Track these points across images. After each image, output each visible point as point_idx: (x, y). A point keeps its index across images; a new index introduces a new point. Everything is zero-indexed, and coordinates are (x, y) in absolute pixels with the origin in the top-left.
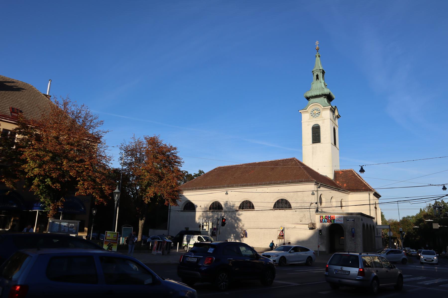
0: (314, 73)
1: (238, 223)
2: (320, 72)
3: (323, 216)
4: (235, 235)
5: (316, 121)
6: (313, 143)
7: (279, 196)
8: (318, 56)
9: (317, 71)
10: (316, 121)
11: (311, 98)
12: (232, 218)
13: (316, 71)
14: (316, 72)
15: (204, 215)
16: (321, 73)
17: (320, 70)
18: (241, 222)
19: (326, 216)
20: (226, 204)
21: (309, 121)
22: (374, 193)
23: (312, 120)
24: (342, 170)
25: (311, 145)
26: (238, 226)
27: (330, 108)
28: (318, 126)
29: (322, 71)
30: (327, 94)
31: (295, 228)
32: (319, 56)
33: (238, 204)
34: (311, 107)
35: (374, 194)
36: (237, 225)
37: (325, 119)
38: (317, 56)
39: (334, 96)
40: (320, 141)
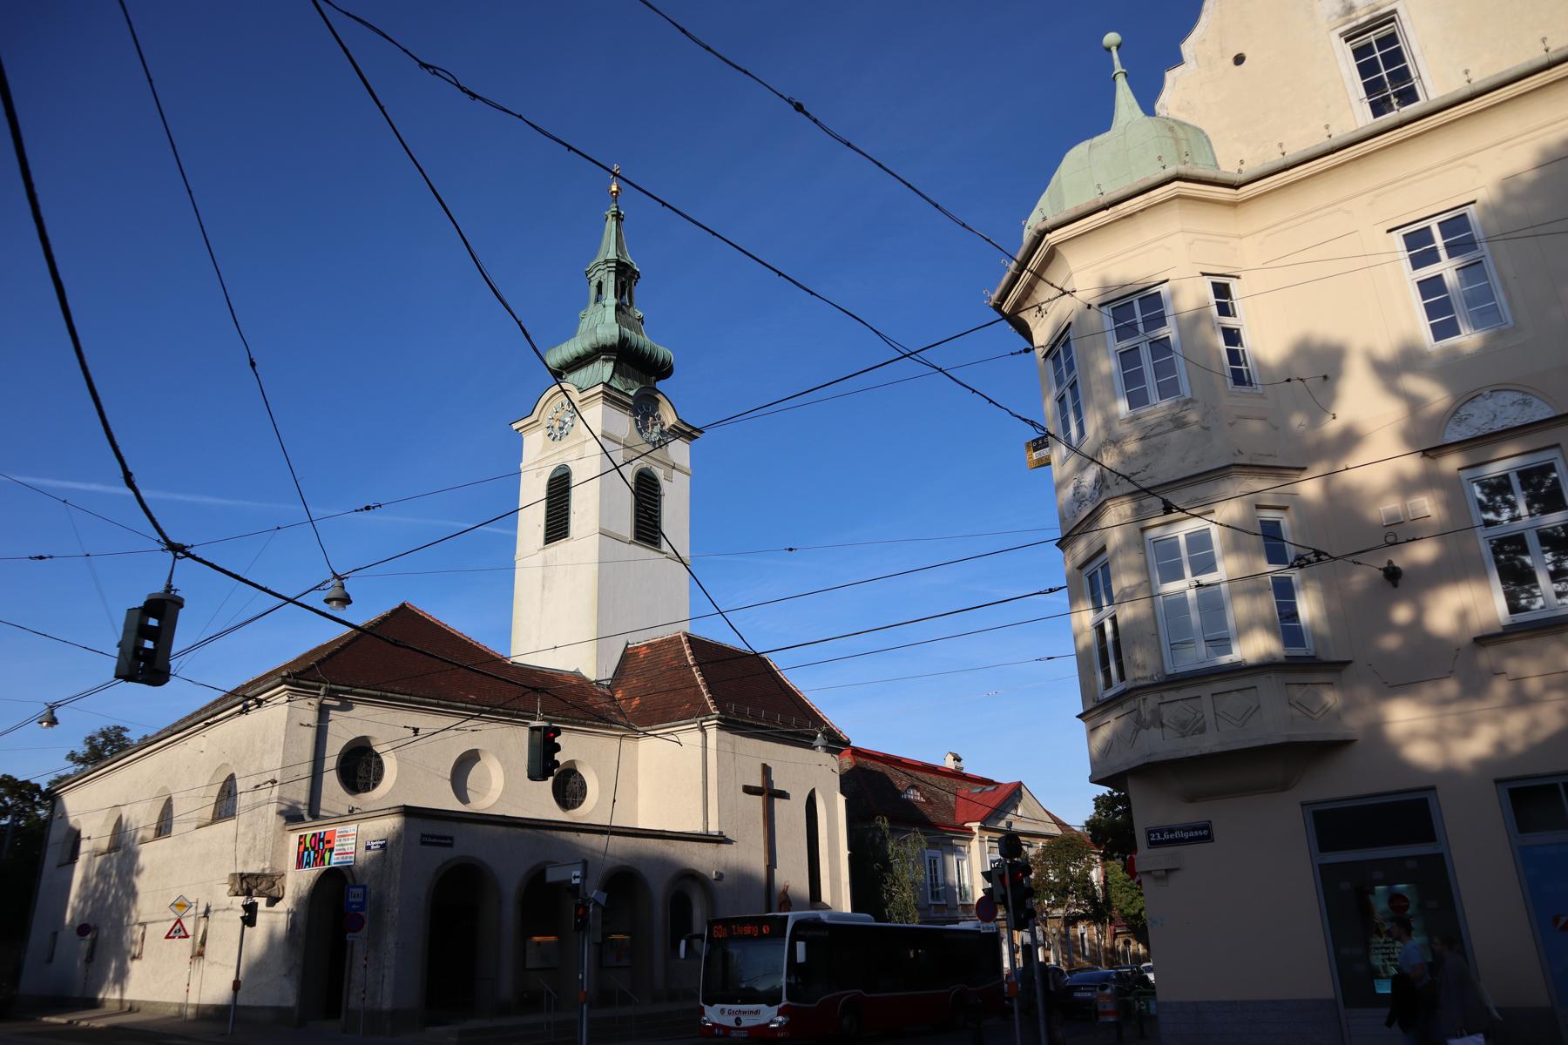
0: (592, 279)
2: (606, 271)
7: (220, 764)
8: (613, 216)
16: (612, 275)
17: (607, 261)
19: (314, 835)
21: (544, 456)
22: (715, 722)
23: (550, 453)
24: (651, 641)
25: (541, 553)
28: (566, 471)
29: (614, 265)
30: (609, 343)
34: (550, 402)
35: (720, 728)
37: (586, 441)
38: (610, 217)
39: (664, 352)
40: (567, 532)
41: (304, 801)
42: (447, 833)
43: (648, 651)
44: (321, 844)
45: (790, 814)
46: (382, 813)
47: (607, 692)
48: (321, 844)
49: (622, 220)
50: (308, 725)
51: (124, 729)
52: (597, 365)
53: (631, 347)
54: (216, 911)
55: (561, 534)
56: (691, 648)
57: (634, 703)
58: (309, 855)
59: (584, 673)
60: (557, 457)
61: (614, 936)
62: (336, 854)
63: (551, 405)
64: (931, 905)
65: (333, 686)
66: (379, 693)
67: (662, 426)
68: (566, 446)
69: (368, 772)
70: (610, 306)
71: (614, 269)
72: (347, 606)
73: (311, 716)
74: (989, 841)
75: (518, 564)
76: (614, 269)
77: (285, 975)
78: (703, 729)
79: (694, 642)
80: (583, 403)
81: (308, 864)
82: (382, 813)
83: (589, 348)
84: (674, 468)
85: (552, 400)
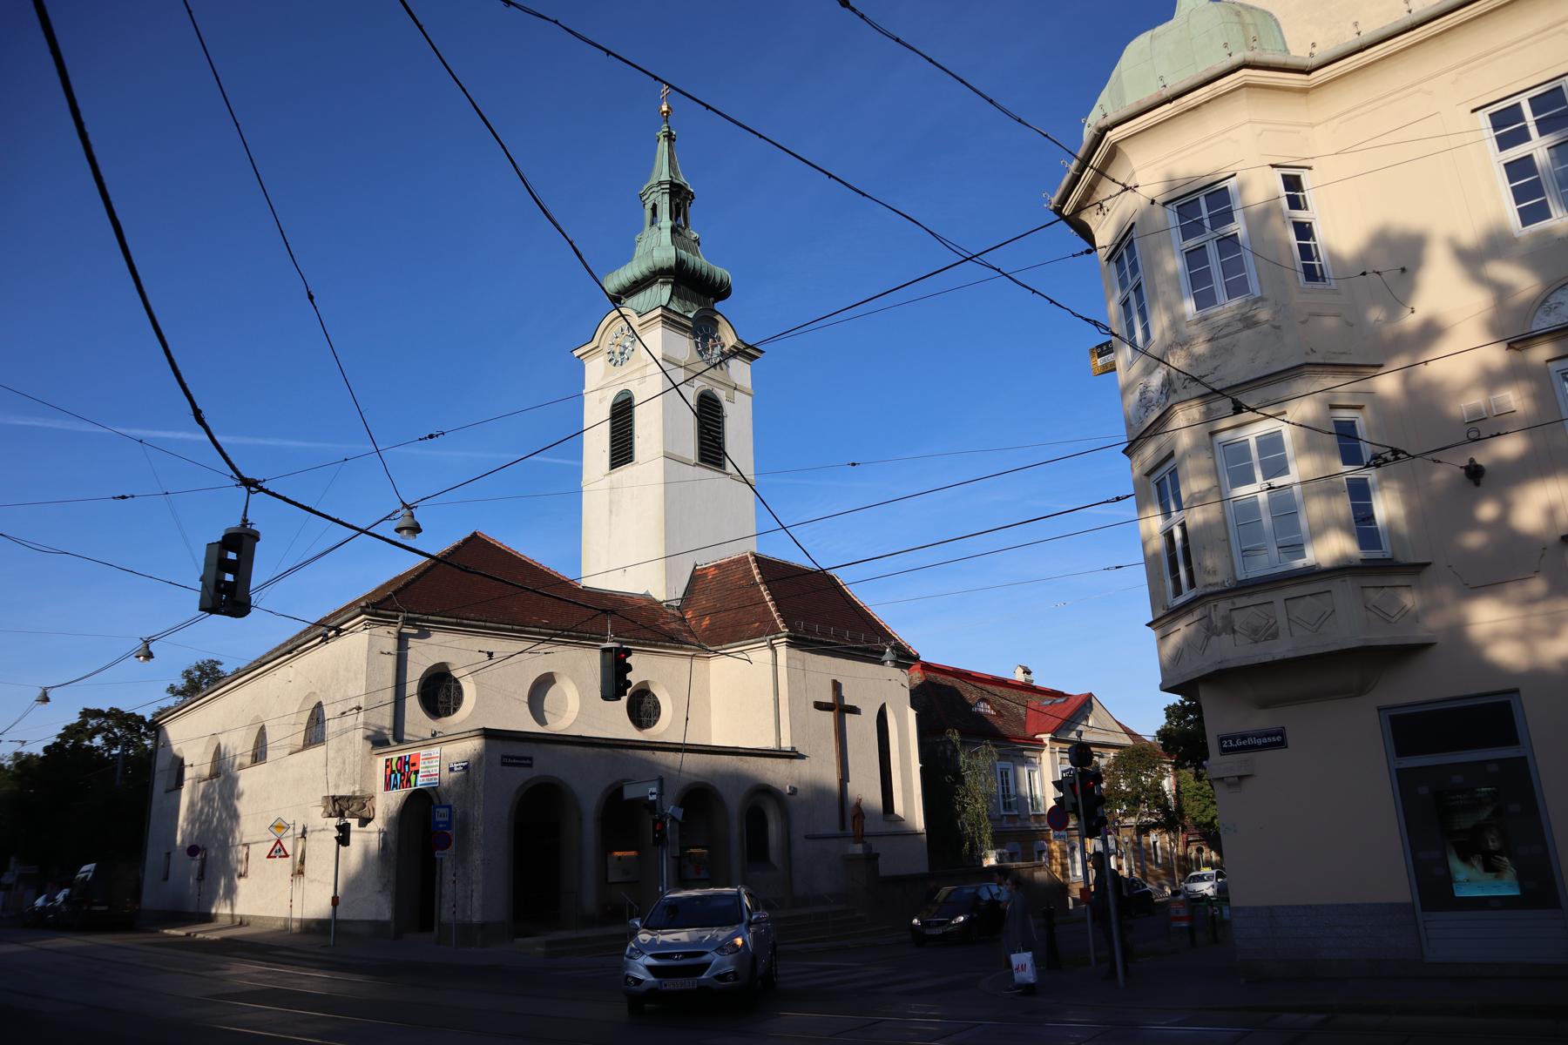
3: (392, 759)
6: (612, 469)
8: (664, 136)
9: (653, 189)
11: (626, 297)
13: (649, 193)
14: (652, 197)
16: (667, 197)
17: (660, 183)
19: (400, 758)
22: (785, 639)
27: (661, 315)
28: (628, 397)
30: (666, 265)
32: (670, 137)
34: (610, 327)
35: (790, 645)
38: (662, 137)
39: (721, 272)
41: (388, 726)
42: (527, 754)
43: (716, 572)
44: (407, 766)
45: (861, 729)
46: (463, 736)
47: (677, 613)
48: (407, 766)
49: (674, 140)
50: (389, 653)
51: (218, 663)
52: (655, 288)
53: (688, 269)
54: (312, 831)
55: (626, 459)
56: (759, 567)
57: (704, 623)
58: (396, 777)
59: (654, 596)
61: (692, 850)
62: (421, 776)
63: (611, 330)
64: (1002, 816)
65: (410, 615)
66: (455, 620)
67: (722, 347)
68: (627, 371)
69: (448, 697)
70: (666, 228)
71: (668, 191)
72: (417, 535)
73: (390, 644)
74: (1059, 752)
75: (584, 489)
76: (668, 191)
77: (380, 891)
78: (772, 647)
79: (759, 560)
80: (642, 327)
81: (395, 786)
82: (463, 736)
83: (646, 272)
84: (735, 389)
85: (612, 325)
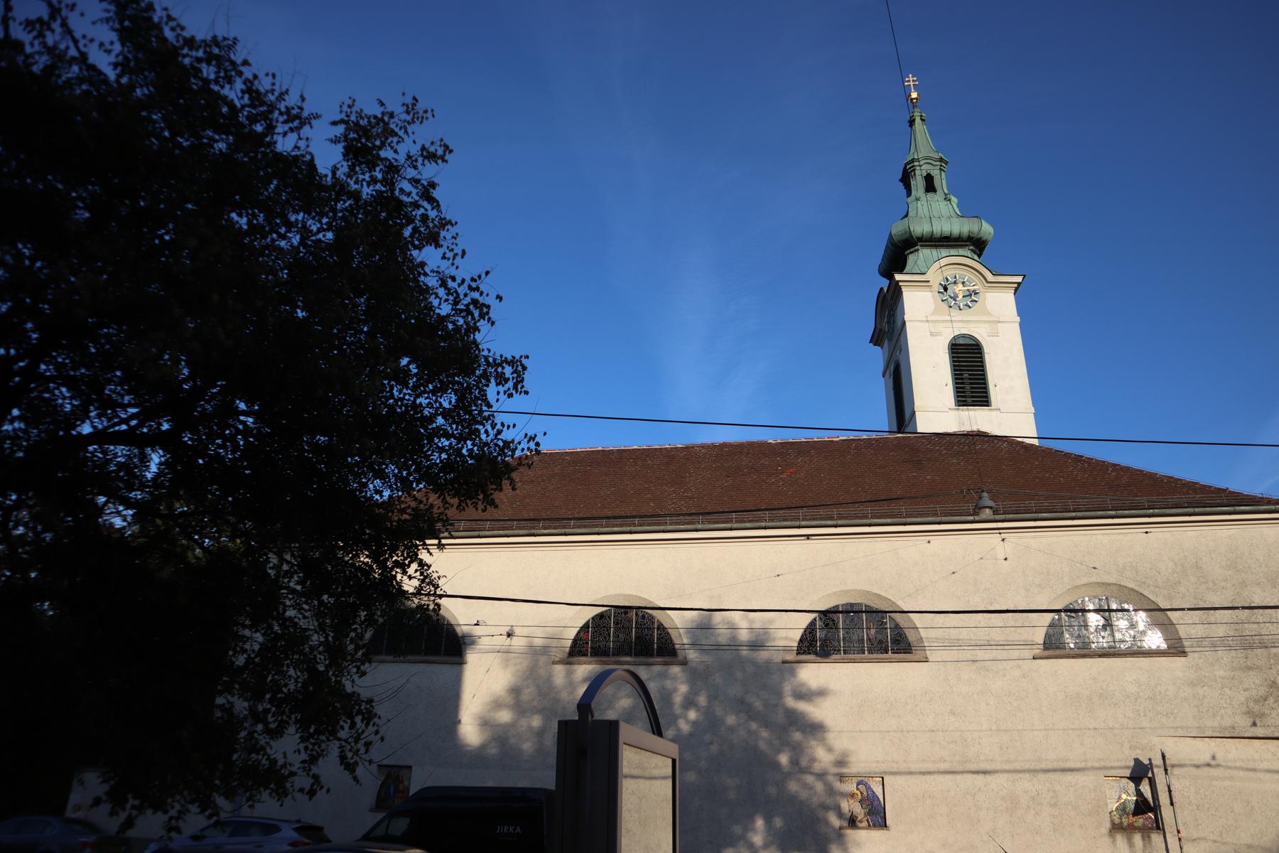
1: (797, 750)
4: (778, 822)
5: (963, 321)
10: (963, 321)
11: (921, 246)
12: (751, 714)
15: (528, 694)
18: (823, 740)
20: (703, 628)
25: (956, 413)
26: (804, 763)
28: (973, 343)
31: (1218, 765)
33: (790, 630)
36: (795, 762)
37: (999, 322)
60: (960, 325)
